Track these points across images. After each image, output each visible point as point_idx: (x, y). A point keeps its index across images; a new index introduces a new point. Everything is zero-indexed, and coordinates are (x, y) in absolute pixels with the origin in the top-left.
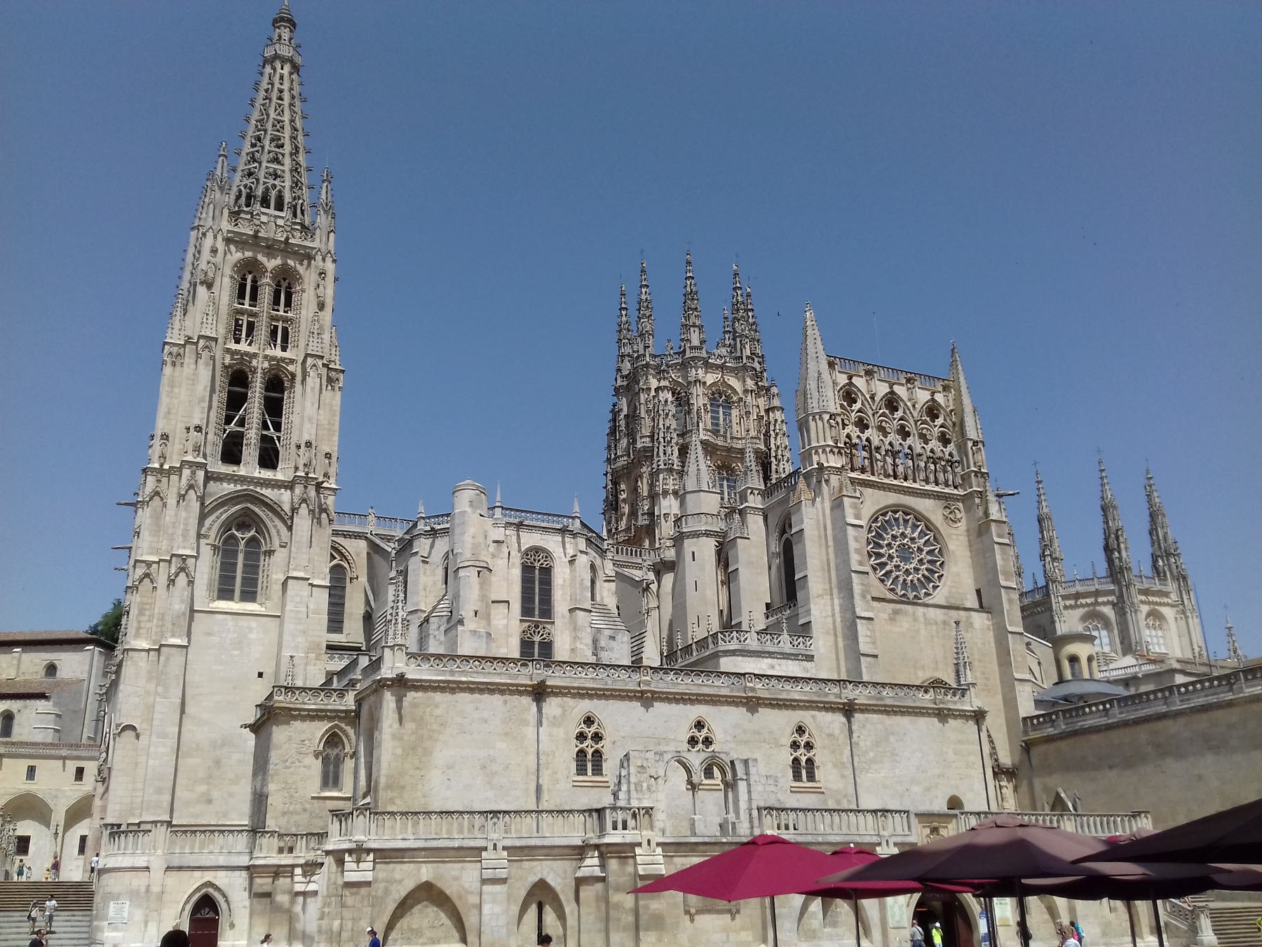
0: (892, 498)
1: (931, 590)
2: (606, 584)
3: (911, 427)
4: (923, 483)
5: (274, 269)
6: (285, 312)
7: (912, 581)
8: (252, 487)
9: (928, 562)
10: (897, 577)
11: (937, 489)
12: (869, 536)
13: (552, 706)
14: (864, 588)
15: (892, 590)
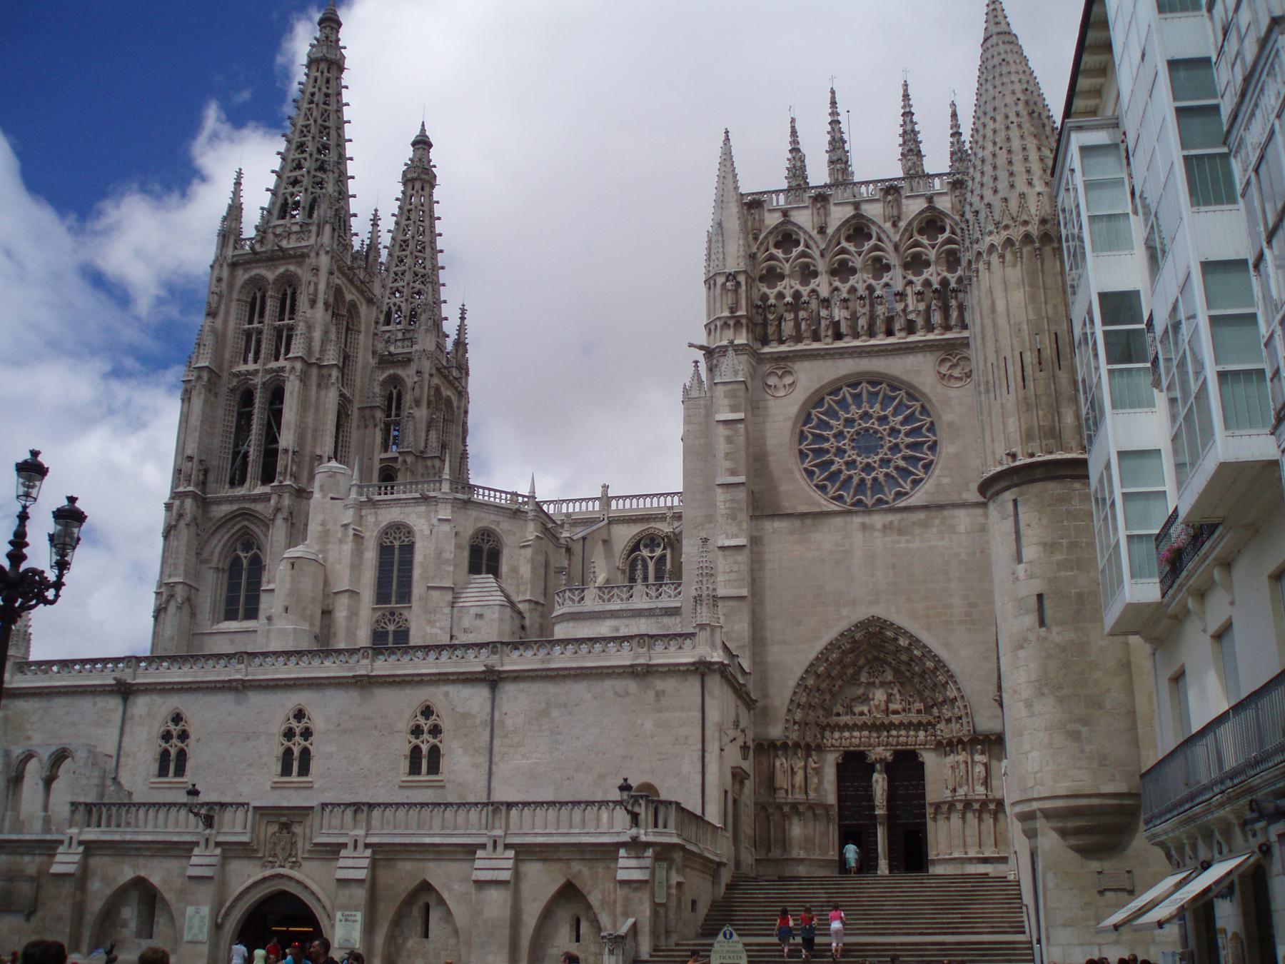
0: (847, 367)
1: (908, 487)
2: (523, 551)
3: (892, 258)
4: (903, 334)
5: (276, 281)
6: (290, 319)
7: (875, 479)
8: (246, 506)
9: (908, 446)
10: (850, 477)
11: (931, 336)
12: (805, 428)
13: (141, 705)
14: (735, 505)
15: (839, 498)
